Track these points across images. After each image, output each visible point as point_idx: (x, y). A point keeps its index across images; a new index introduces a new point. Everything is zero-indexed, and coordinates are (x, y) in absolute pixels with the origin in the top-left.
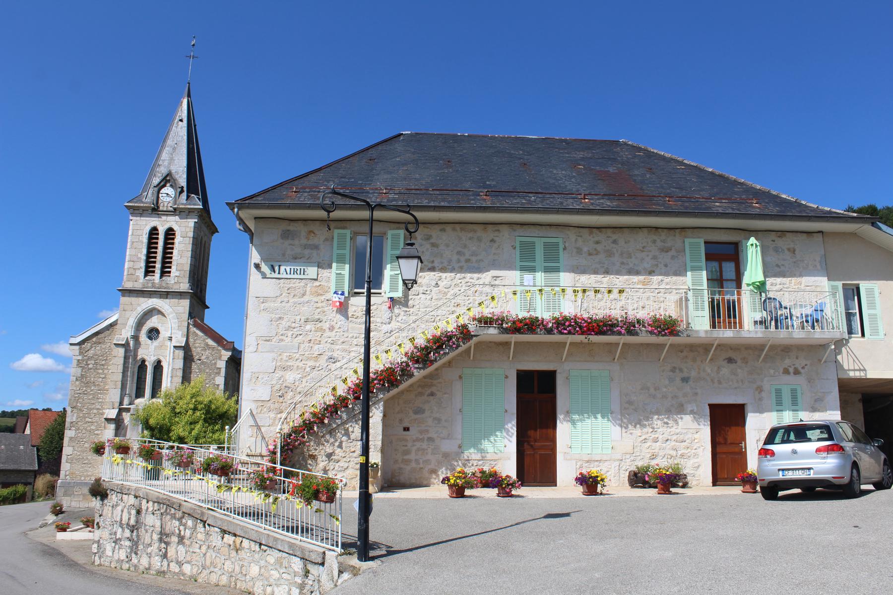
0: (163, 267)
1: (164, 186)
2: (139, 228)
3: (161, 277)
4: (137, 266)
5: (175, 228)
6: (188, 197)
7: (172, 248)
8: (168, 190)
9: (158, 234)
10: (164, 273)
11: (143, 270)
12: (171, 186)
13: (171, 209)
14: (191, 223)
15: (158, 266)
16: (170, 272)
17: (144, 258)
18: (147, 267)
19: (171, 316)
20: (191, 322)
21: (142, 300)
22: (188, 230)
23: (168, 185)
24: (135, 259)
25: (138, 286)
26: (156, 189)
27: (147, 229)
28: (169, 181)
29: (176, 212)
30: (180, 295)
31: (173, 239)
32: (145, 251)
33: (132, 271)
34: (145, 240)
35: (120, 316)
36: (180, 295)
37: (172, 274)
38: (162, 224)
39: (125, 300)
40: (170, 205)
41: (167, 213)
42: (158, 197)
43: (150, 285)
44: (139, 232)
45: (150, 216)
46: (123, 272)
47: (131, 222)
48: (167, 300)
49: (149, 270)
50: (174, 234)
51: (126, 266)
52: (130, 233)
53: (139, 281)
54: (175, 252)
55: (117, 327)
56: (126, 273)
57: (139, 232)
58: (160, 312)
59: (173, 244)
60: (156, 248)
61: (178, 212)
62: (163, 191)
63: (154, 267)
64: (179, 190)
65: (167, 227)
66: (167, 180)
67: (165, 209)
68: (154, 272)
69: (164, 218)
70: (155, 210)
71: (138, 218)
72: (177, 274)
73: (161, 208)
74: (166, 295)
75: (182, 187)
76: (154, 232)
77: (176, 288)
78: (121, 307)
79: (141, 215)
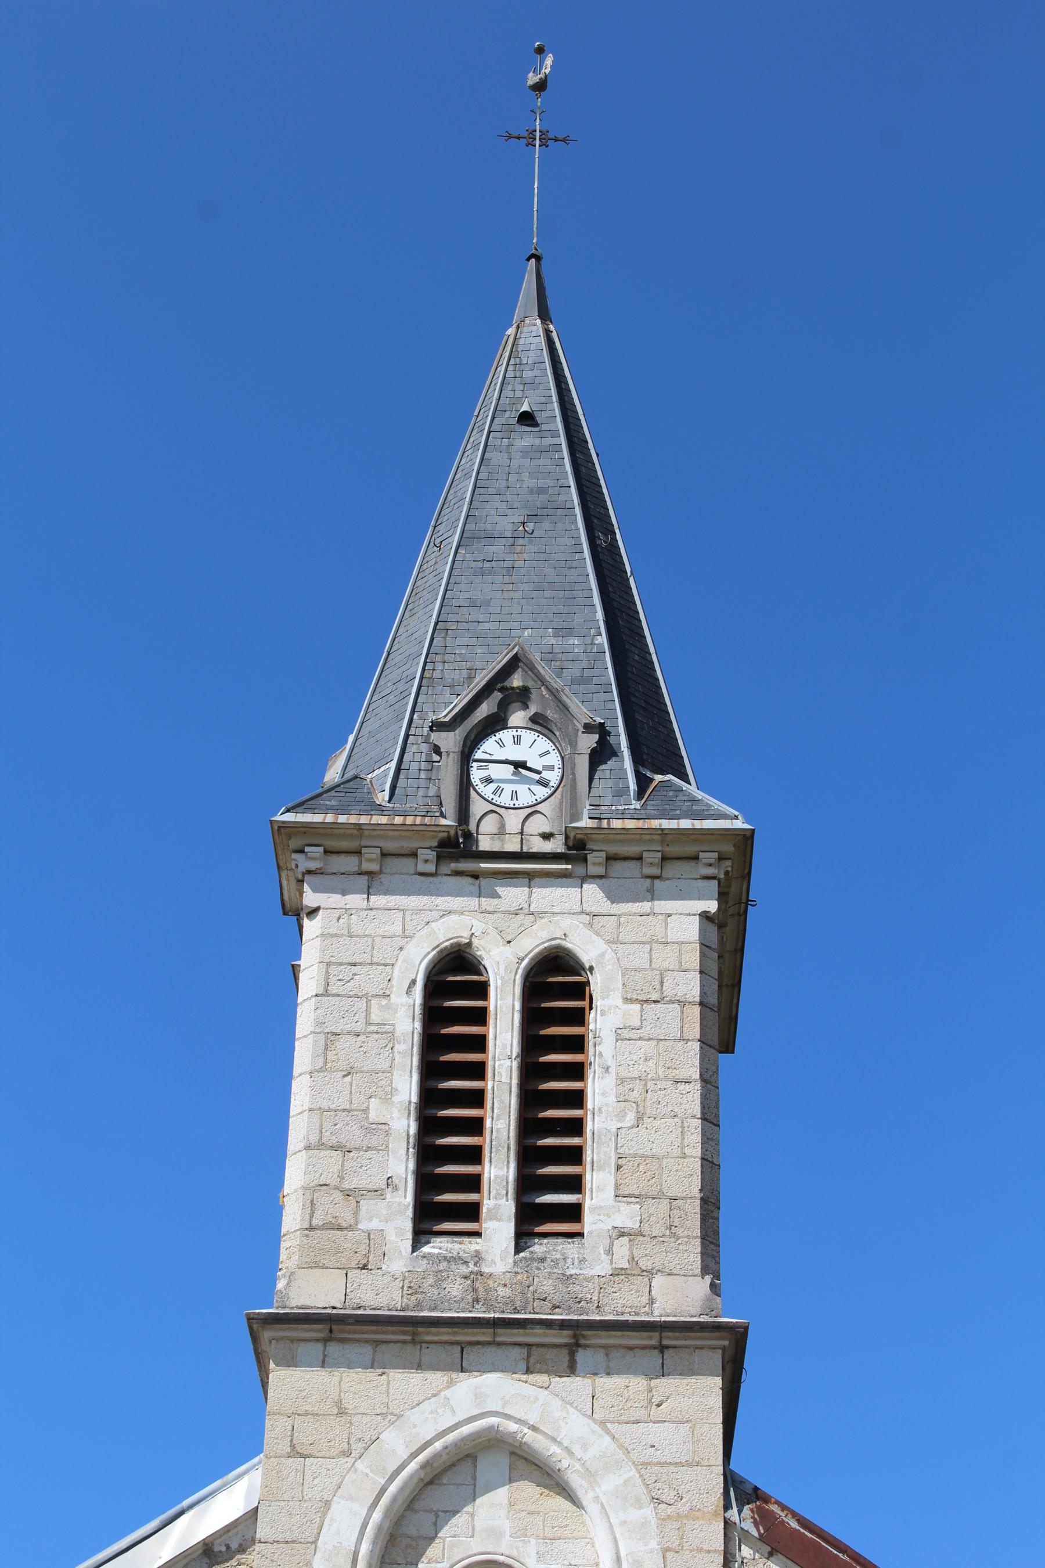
0: (527, 1184)
1: (495, 723)
2: (360, 963)
3: (523, 1236)
4: (365, 1174)
5: (586, 947)
6: (643, 783)
7: (577, 1071)
8: (519, 742)
9: (481, 990)
10: (547, 1206)
11: (405, 1198)
12: (539, 723)
13: (557, 845)
14: (680, 921)
15: (499, 1171)
16: (574, 1213)
17: (404, 1125)
18: (427, 1183)
19: (609, 1483)
20: (745, 1519)
21: (405, 1383)
22: (666, 958)
23: (518, 717)
24: (352, 1135)
25: (380, 1293)
26: (450, 741)
27: (415, 961)
28: (523, 696)
29: (576, 855)
30: (659, 1343)
31: (578, 1017)
32: (407, 1087)
33: (332, 1206)
34: (405, 1017)
35: (270, 1492)
36: (659, 1343)
37: (590, 1221)
38: (507, 933)
39: (292, 1385)
40: (538, 825)
41: (523, 865)
42: (465, 785)
43: (456, 1288)
44: (368, 980)
45: (426, 881)
46: (277, 1212)
47: (311, 927)
48: (577, 1385)
49: (442, 1202)
50: (580, 990)
51: (296, 1174)
52: (308, 983)
53: (390, 1265)
54: (599, 1090)
55: (254, 1556)
56: (292, 1218)
57: (368, 980)
58: (526, 1464)
59: (578, 1044)
60: (478, 1071)
61: (595, 860)
62: (489, 747)
63: (474, 1183)
64: (588, 742)
65: (532, 943)
66: (502, 696)
67: (512, 845)
68: (472, 1212)
69: (512, 895)
70: (457, 853)
71: (356, 900)
72: (627, 1216)
73: (485, 844)
74: (569, 1343)
75: (602, 731)
76: (453, 982)
77: (624, 1303)
78: (275, 1430)
79: (371, 882)
